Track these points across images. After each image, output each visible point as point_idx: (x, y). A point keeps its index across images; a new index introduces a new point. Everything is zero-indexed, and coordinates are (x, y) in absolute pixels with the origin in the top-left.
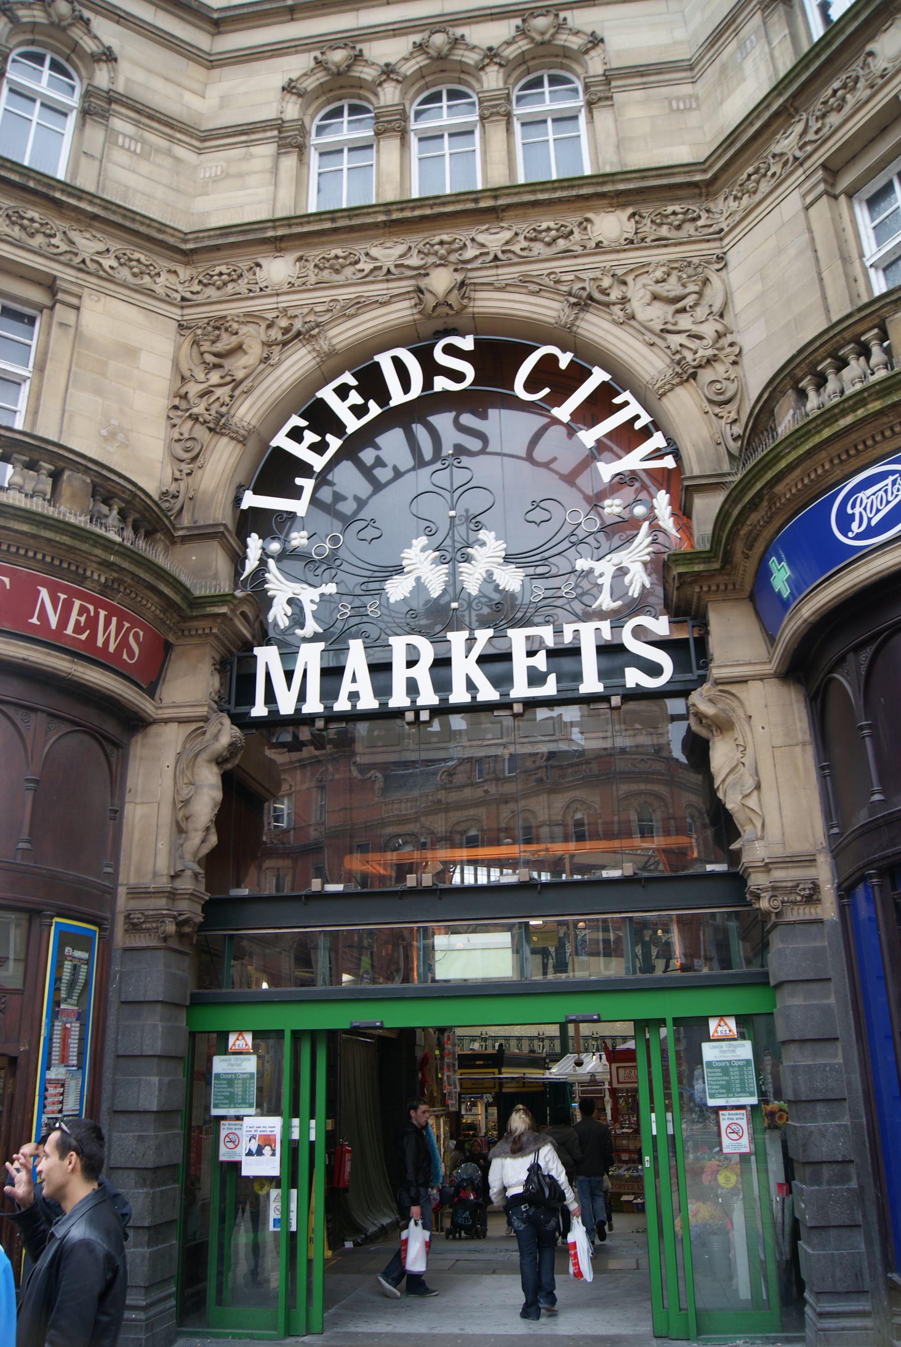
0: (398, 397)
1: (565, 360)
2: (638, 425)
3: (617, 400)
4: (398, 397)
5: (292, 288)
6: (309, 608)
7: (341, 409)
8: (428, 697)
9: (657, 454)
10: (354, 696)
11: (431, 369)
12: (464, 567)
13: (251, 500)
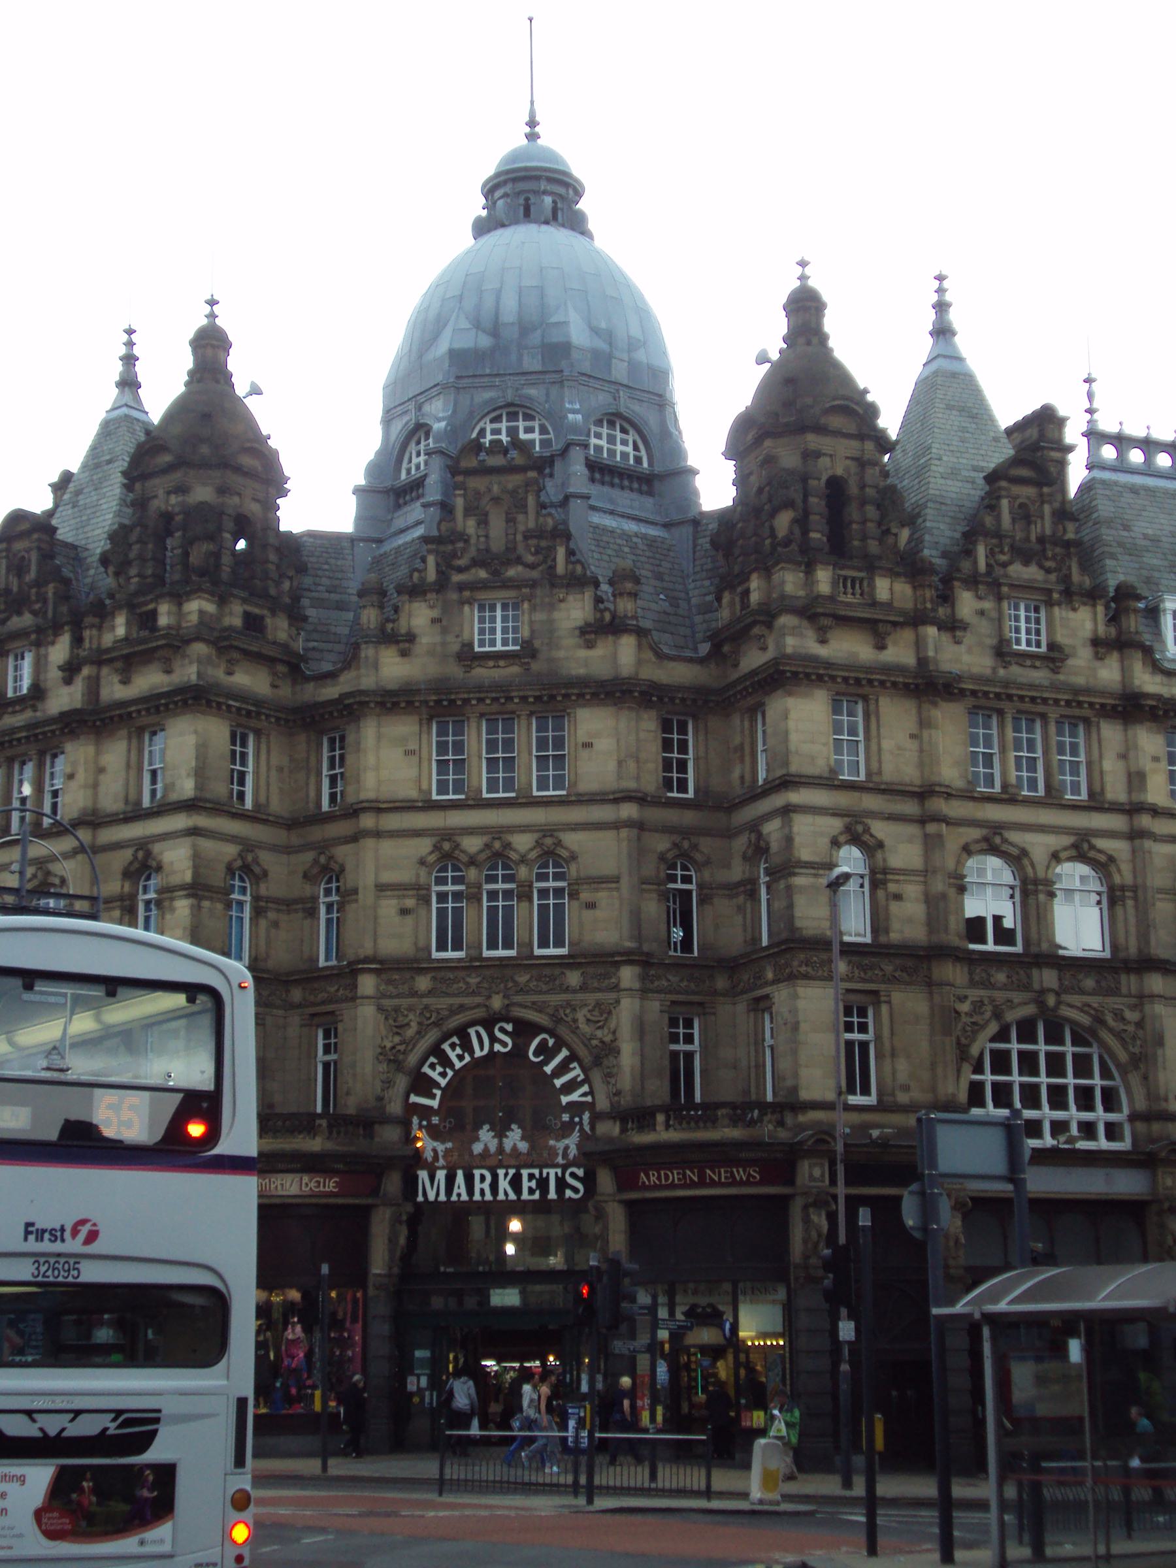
0: (478, 1053)
1: (551, 1042)
2: (579, 1079)
3: (572, 1066)
4: (478, 1053)
5: (431, 993)
6: (441, 1154)
7: (452, 1055)
8: (488, 1197)
9: (585, 1095)
10: (459, 1195)
11: (493, 1039)
12: (505, 1140)
13: (414, 1099)
